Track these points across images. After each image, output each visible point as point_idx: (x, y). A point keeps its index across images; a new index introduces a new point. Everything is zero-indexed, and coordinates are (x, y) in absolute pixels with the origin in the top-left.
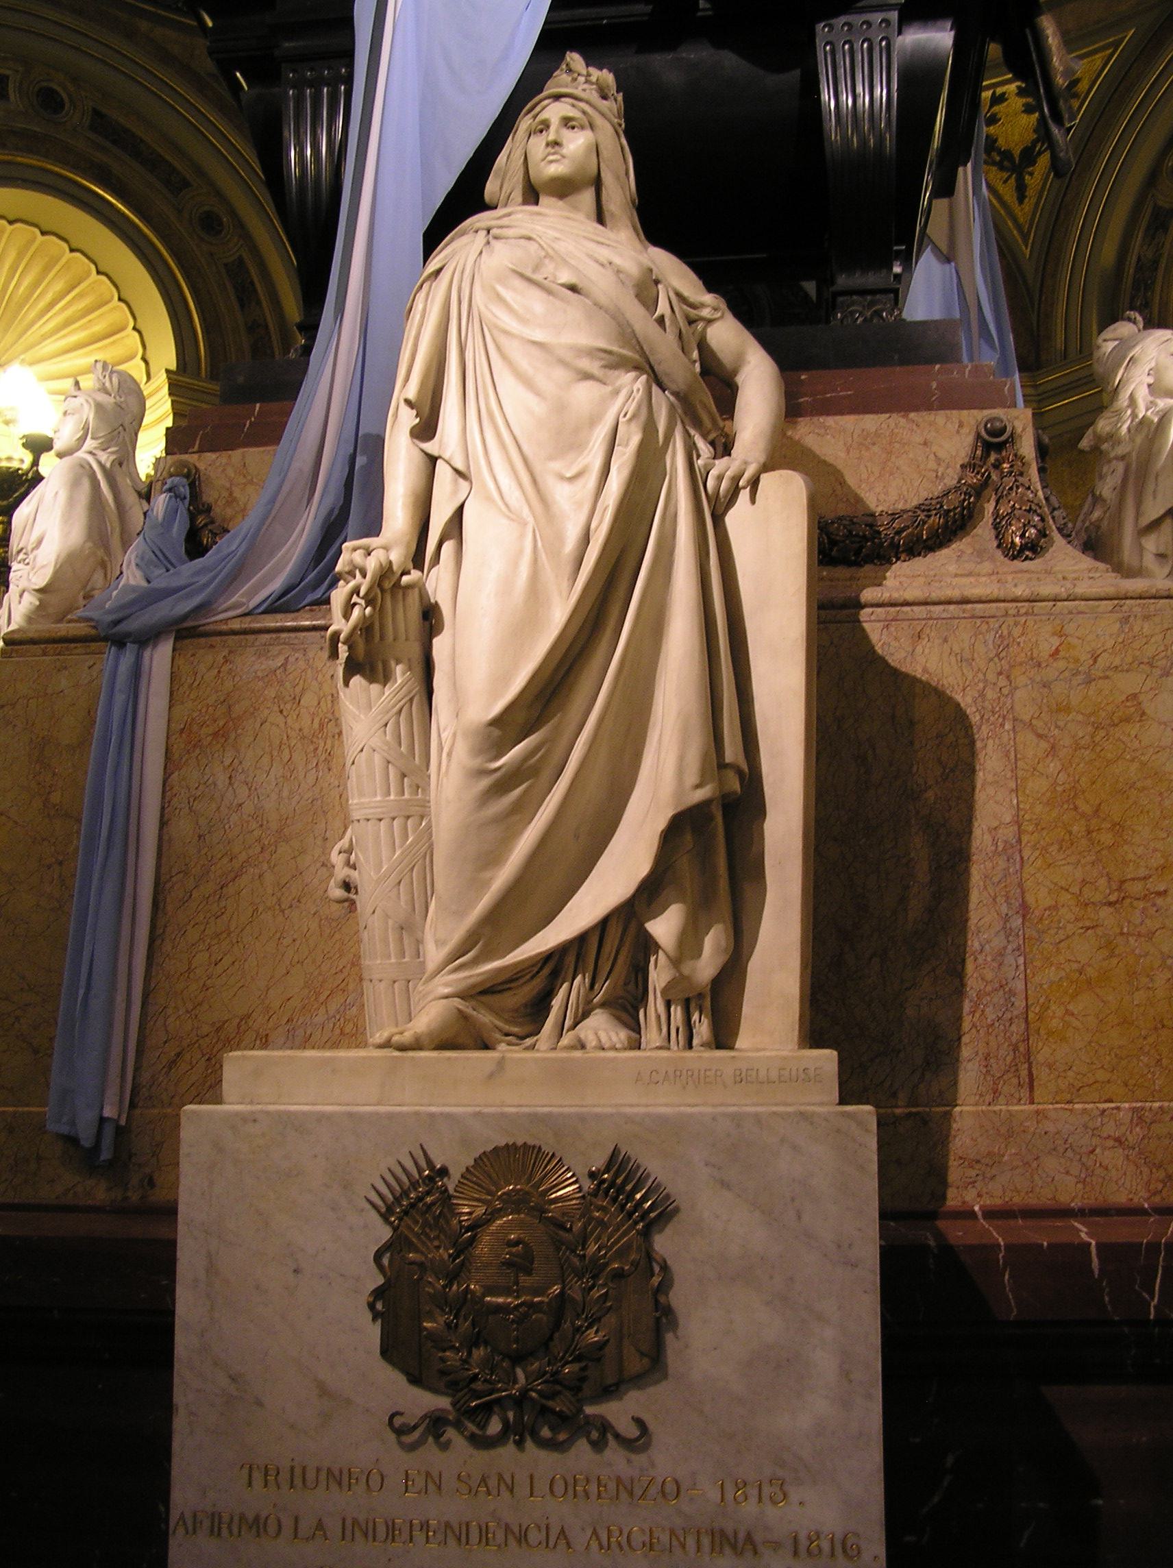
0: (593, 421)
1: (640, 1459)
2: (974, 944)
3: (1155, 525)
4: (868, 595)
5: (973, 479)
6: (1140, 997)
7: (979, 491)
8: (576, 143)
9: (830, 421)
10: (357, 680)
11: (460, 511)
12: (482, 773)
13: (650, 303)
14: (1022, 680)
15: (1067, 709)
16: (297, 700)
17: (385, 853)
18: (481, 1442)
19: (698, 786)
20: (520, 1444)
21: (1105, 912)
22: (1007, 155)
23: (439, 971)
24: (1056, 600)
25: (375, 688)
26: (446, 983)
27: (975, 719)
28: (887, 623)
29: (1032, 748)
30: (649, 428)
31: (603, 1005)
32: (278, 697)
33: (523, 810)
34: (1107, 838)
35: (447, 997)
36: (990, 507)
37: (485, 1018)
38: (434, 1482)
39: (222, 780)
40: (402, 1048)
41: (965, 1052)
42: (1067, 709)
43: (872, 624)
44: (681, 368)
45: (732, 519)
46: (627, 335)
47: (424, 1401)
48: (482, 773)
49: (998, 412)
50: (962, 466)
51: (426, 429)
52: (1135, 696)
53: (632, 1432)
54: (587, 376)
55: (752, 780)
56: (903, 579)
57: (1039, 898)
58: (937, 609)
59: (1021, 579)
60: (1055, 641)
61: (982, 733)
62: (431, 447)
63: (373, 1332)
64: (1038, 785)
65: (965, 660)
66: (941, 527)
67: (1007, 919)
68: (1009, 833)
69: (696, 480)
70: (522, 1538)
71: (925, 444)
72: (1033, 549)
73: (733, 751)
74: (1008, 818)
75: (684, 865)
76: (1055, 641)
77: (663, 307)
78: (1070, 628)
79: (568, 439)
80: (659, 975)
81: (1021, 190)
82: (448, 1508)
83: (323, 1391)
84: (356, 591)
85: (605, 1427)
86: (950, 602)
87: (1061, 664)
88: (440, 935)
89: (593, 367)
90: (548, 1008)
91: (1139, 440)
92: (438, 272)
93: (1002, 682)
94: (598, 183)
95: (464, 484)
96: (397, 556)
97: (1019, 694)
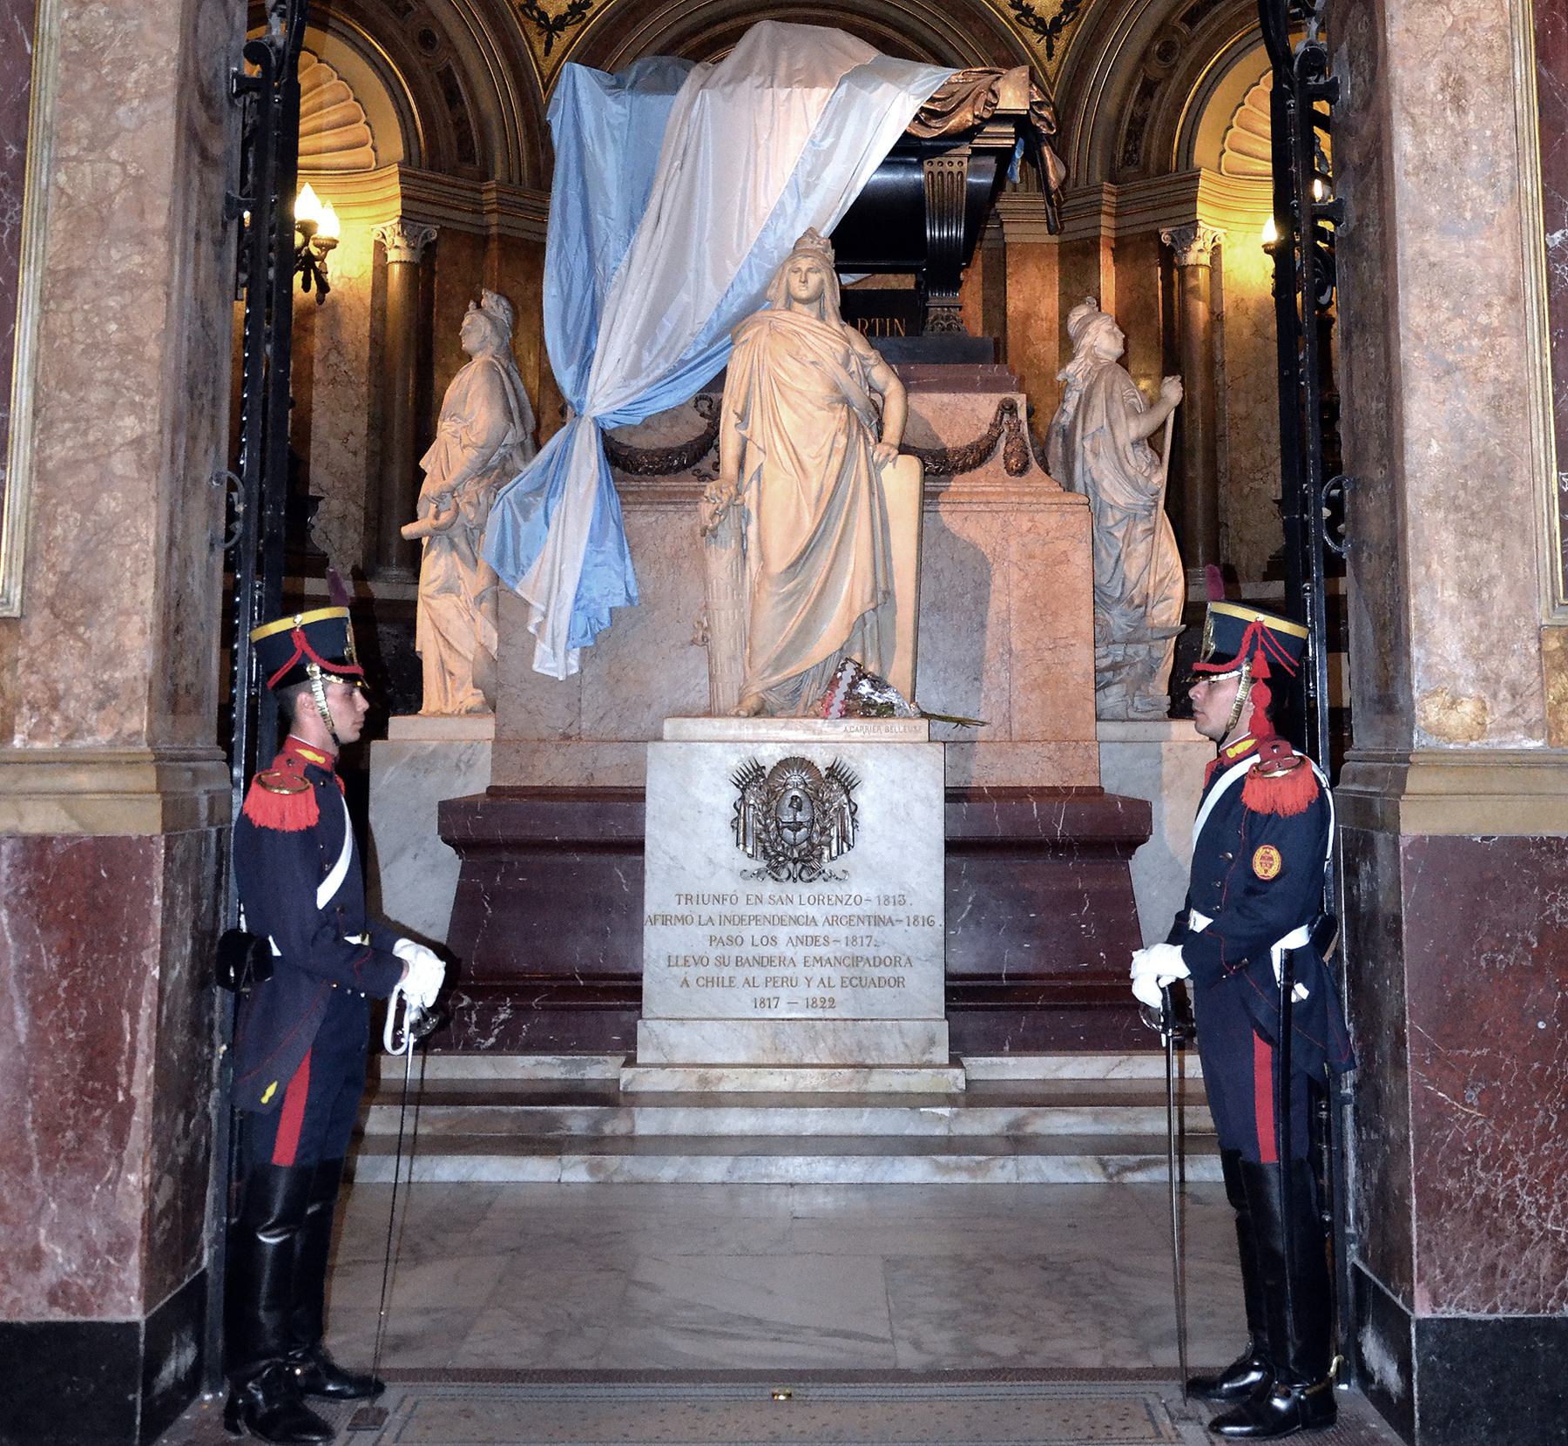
9: (925, 395)
16: (663, 539)
22: (1041, 21)
66: (980, 454)
68: (1004, 615)
70: (796, 921)
81: (1050, 48)
82: (767, 910)
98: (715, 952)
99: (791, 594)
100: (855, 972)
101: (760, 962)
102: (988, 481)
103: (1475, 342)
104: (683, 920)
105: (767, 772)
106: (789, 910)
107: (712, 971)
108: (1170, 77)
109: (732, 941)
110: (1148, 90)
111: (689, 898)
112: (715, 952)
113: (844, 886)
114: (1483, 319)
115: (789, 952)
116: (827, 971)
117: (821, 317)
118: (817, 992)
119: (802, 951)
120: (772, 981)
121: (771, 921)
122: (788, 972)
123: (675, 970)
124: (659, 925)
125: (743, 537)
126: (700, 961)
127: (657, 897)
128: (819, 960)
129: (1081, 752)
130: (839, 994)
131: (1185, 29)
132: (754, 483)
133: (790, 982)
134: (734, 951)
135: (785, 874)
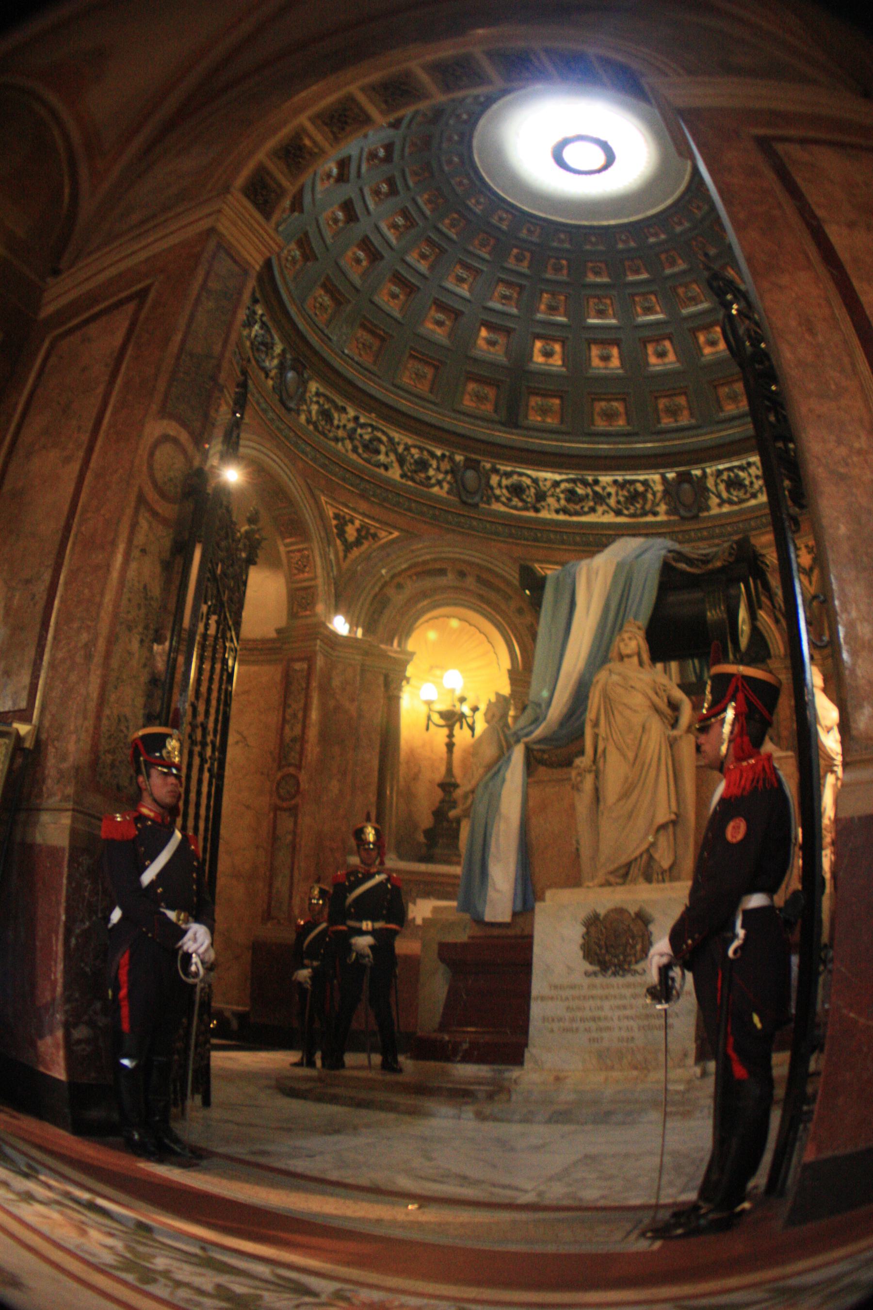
1: (643, 978)
22: (804, 569)
37: (612, 879)
38: (594, 986)
62: (596, 731)
63: (581, 954)
70: (615, 997)
82: (599, 992)
83: (569, 967)
98: (568, 1015)
100: (646, 1022)
101: (594, 1019)
103: (855, 459)
104: (552, 998)
106: (612, 992)
107: (567, 1024)
109: (579, 1009)
111: (556, 987)
112: (568, 1015)
114: (857, 445)
115: (609, 1014)
116: (631, 1023)
118: (624, 1034)
119: (617, 1013)
120: (600, 1029)
121: (601, 998)
122: (609, 1024)
123: (546, 1024)
124: (539, 1002)
126: (560, 1020)
127: (538, 986)
128: (627, 1018)
130: (637, 1034)
133: (609, 1029)
134: (579, 1014)
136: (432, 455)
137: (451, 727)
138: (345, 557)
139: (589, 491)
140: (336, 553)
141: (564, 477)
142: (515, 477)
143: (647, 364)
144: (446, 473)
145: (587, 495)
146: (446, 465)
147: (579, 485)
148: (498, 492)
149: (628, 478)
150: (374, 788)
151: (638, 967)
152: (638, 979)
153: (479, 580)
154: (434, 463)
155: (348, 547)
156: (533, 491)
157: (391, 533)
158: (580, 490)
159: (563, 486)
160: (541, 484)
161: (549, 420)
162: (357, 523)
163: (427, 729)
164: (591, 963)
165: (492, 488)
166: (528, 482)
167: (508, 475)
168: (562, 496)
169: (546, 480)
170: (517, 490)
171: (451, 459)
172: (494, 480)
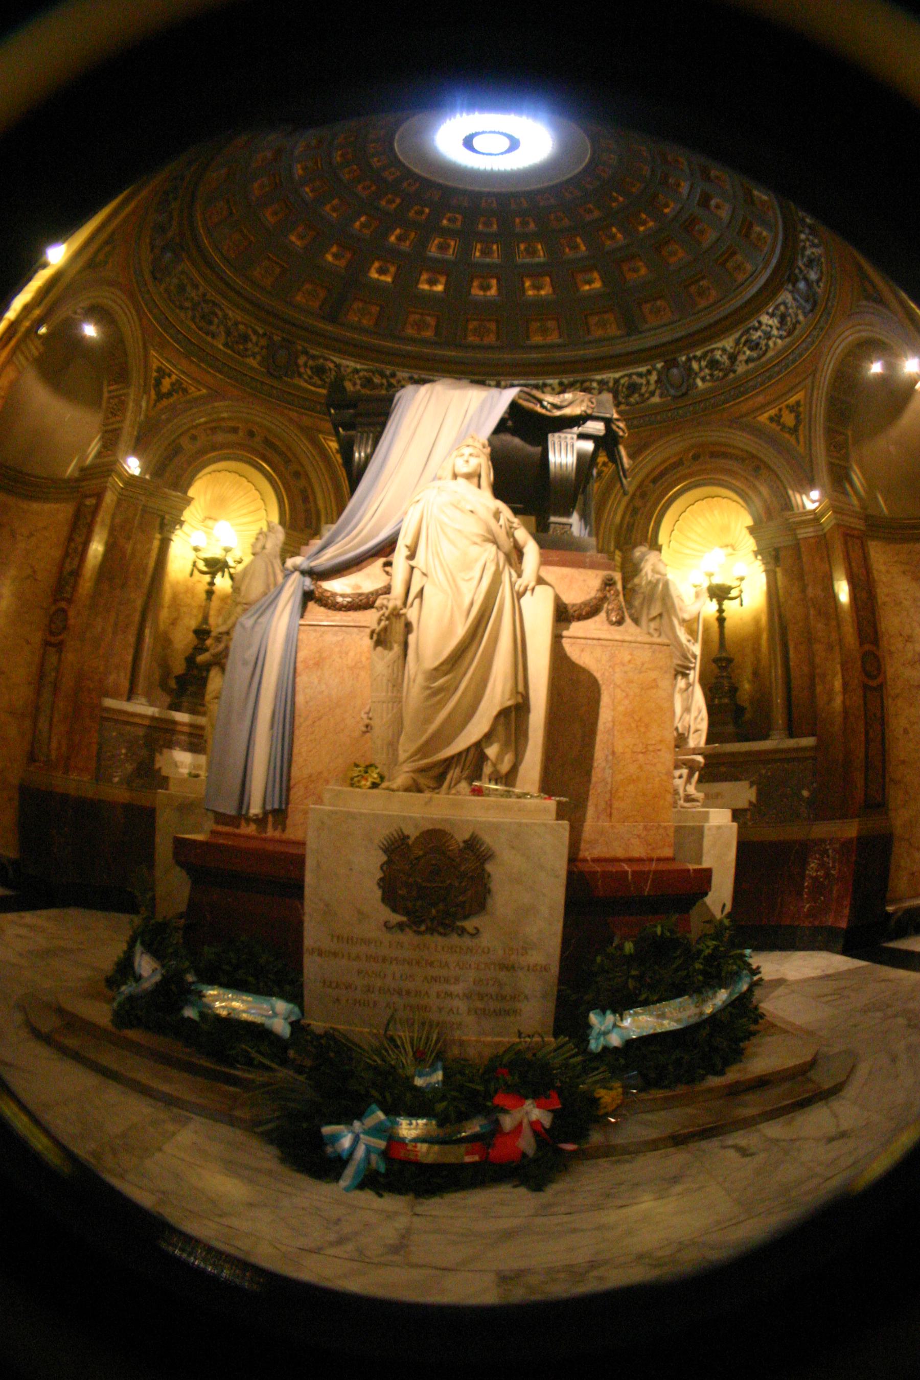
0: (476, 560)
2: (595, 764)
3: (654, 618)
4: (565, 633)
5: (599, 595)
6: (650, 786)
7: (604, 599)
8: (474, 462)
10: (379, 649)
11: (422, 590)
12: (428, 688)
13: (498, 520)
14: (617, 670)
15: (632, 682)
16: (347, 653)
17: (385, 715)
18: (418, 933)
19: (509, 699)
20: (432, 934)
21: (641, 755)
23: (405, 762)
24: (630, 642)
25: (386, 652)
26: (407, 767)
27: (601, 682)
28: (572, 644)
29: (619, 694)
30: (498, 565)
31: (465, 779)
32: (340, 652)
33: (442, 704)
34: (643, 729)
35: (407, 772)
36: (605, 606)
37: (422, 781)
39: (316, 681)
40: (393, 790)
41: (590, 803)
42: (632, 682)
43: (566, 643)
44: (507, 544)
45: (523, 600)
46: (490, 531)
47: (397, 918)
48: (428, 688)
49: (609, 572)
50: (598, 591)
51: (412, 556)
52: (655, 680)
53: (474, 932)
54: (475, 543)
55: (526, 697)
56: (576, 628)
57: (619, 749)
58: (590, 642)
59: (617, 633)
60: (629, 657)
61: (603, 688)
62: (413, 563)
63: (379, 893)
64: (621, 708)
65: (598, 661)
66: (590, 611)
67: (607, 756)
68: (610, 725)
69: (512, 585)
71: (584, 581)
72: (620, 622)
73: (521, 688)
74: (610, 719)
75: (501, 729)
76: (629, 657)
77: (502, 522)
78: (635, 653)
79: (467, 566)
80: (487, 769)
83: (359, 912)
84: (383, 615)
85: (462, 931)
86: (594, 639)
87: (631, 666)
88: (405, 749)
89: (478, 540)
90: (445, 778)
91: (649, 588)
92: (418, 501)
93: (611, 670)
94: (479, 476)
95: (425, 578)
96: (399, 603)
97: (617, 675)
99: (441, 689)
102: (595, 627)
105: (410, 842)
108: (645, 506)
110: (635, 511)
113: (476, 941)
117: (479, 486)
125: (406, 645)
129: (661, 831)
131: (651, 485)
132: (417, 601)
135: (423, 928)
136: (255, 332)
137: (213, 575)
138: (155, 405)
139: (384, 381)
140: (148, 402)
141: (363, 367)
142: (321, 361)
143: (469, 293)
144: (262, 348)
145: (382, 385)
146: (263, 342)
147: (377, 376)
148: (302, 370)
149: (423, 376)
150: (133, 630)
151: (469, 924)
152: (467, 941)
153: (266, 441)
154: (254, 338)
155: (160, 396)
156: (334, 373)
157: (199, 390)
158: (377, 380)
159: (361, 374)
160: (342, 369)
161: (365, 322)
162: (174, 377)
163: (191, 575)
164: (395, 910)
165: (298, 366)
166: (332, 366)
167: (314, 357)
168: (359, 382)
169: (348, 366)
170: (320, 371)
171: (270, 338)
172: (302, 360)
